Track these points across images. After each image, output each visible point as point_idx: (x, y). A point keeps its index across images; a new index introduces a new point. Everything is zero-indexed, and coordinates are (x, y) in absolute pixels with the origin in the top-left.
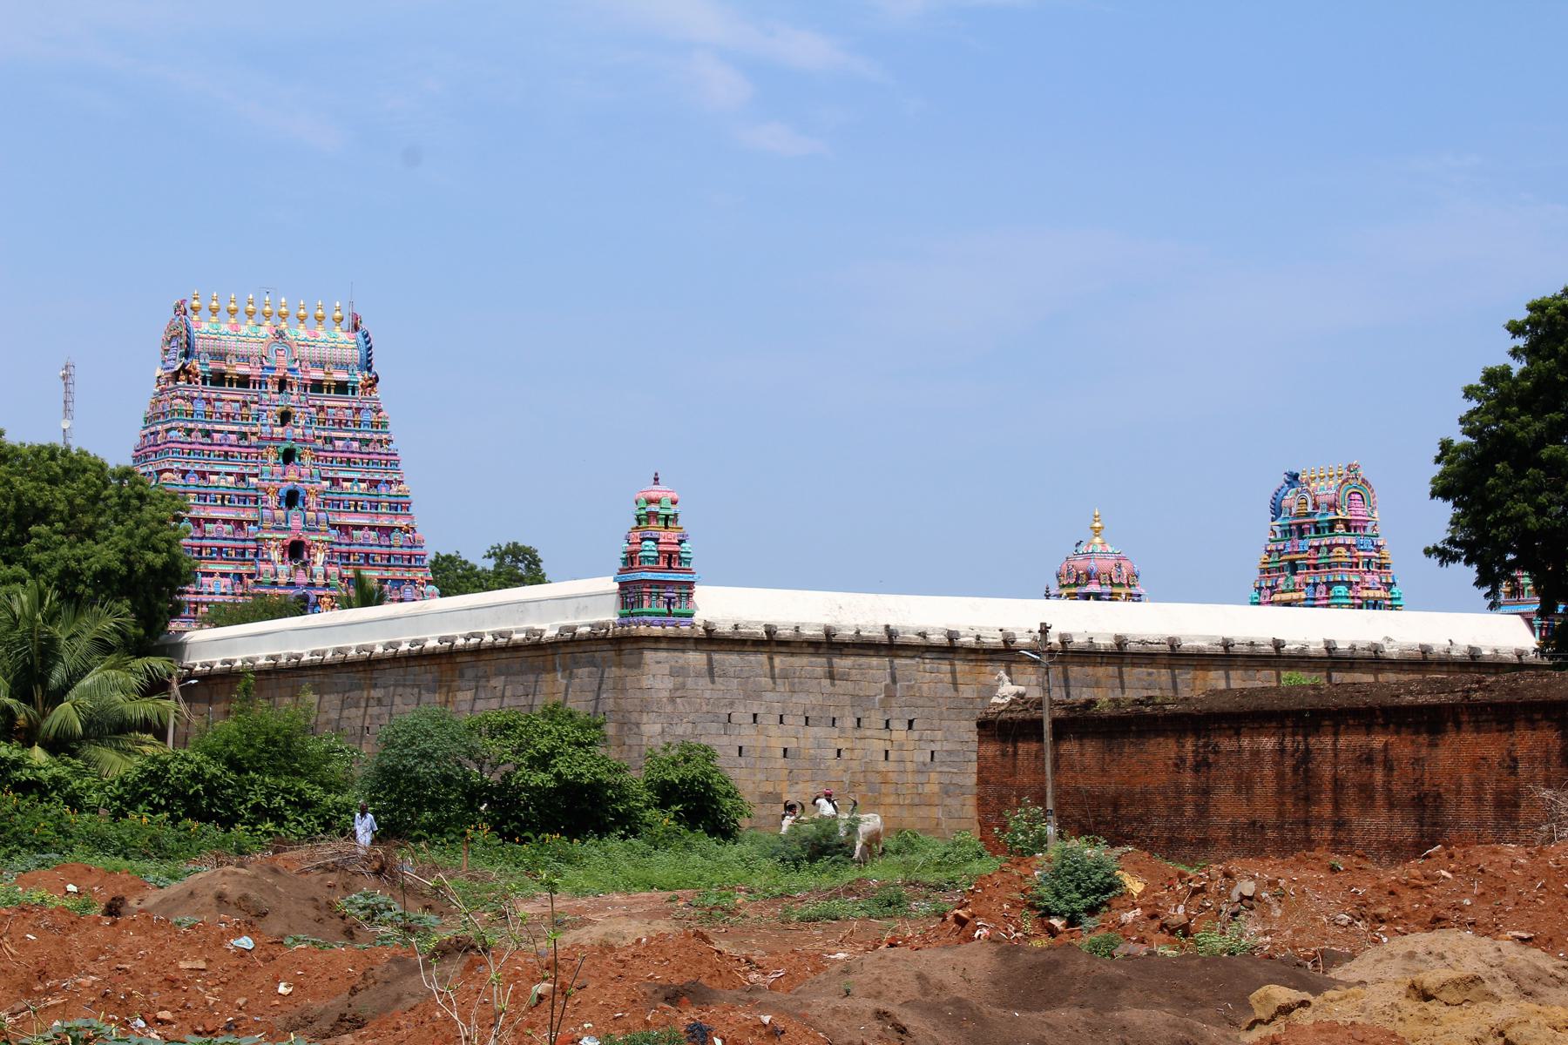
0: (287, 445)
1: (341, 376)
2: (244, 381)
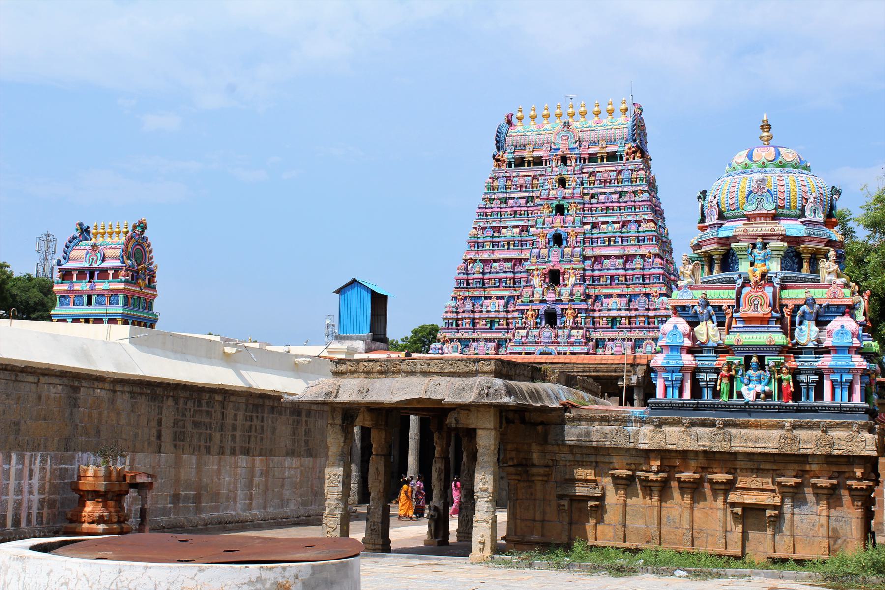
0: (556, 202)
1: (611, 149)
2: (538, 162)
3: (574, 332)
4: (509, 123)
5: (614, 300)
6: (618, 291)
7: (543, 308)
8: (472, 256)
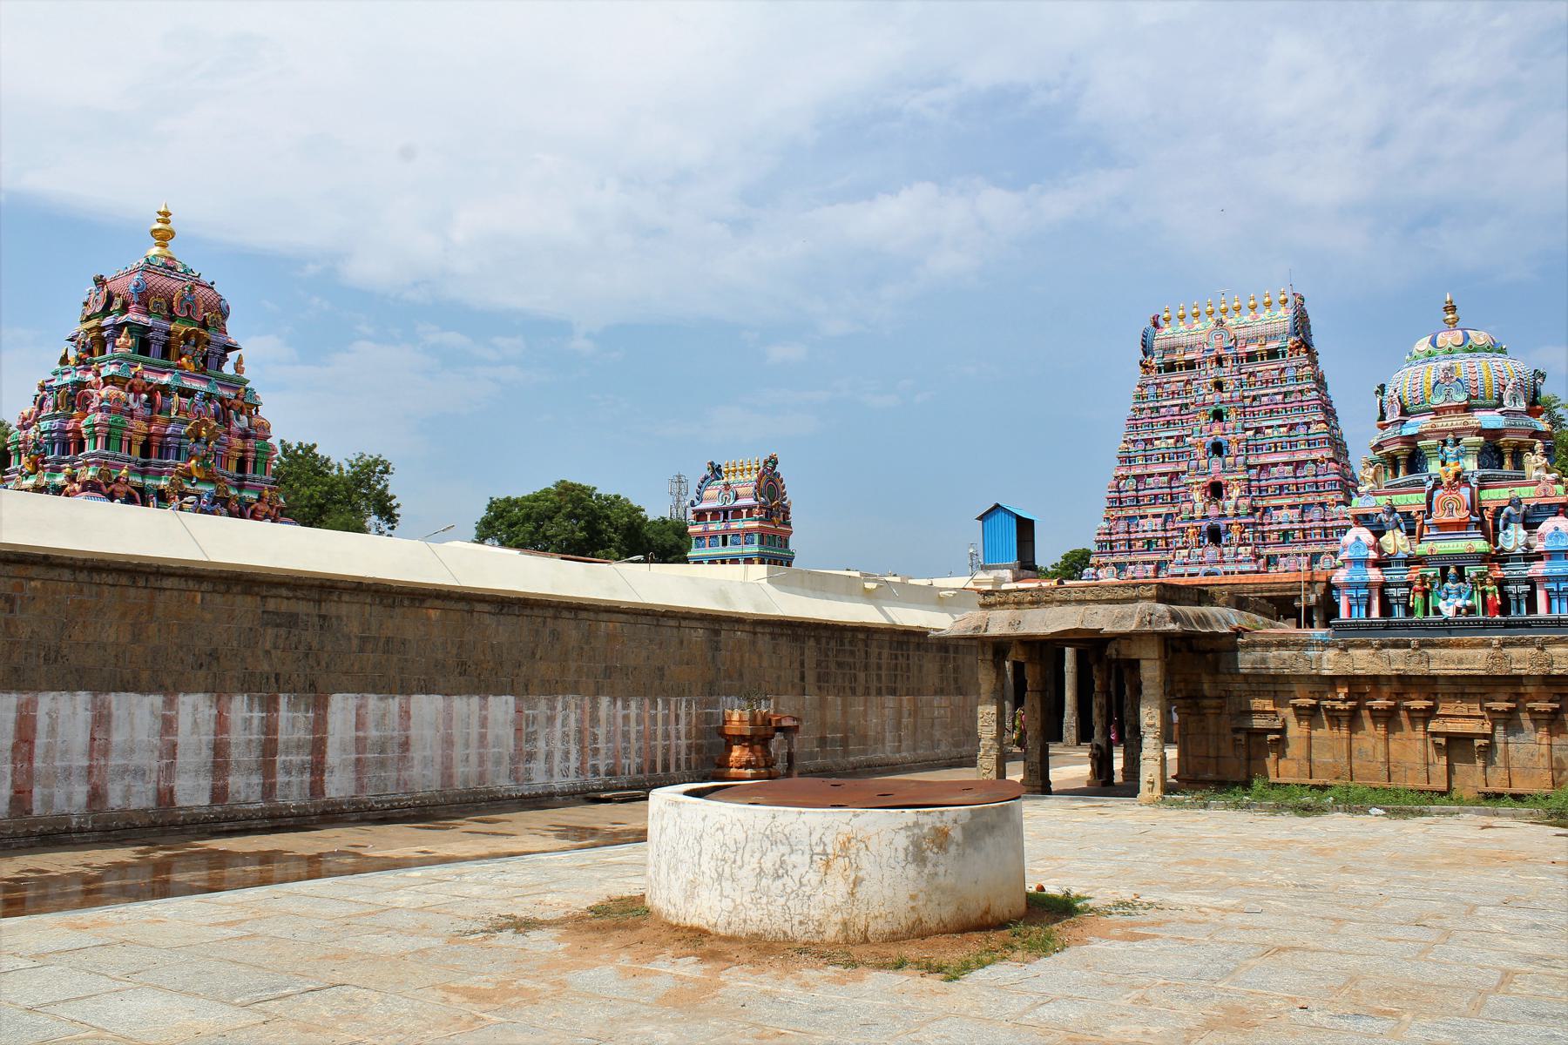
1: (1272, 345)
2: (1190, 365)
3: (1241, 549)
4: (1156, 325)
5: (1285, 512)
6: (1289, 501)
7: (1205, 525)
8: (1124, 472)
